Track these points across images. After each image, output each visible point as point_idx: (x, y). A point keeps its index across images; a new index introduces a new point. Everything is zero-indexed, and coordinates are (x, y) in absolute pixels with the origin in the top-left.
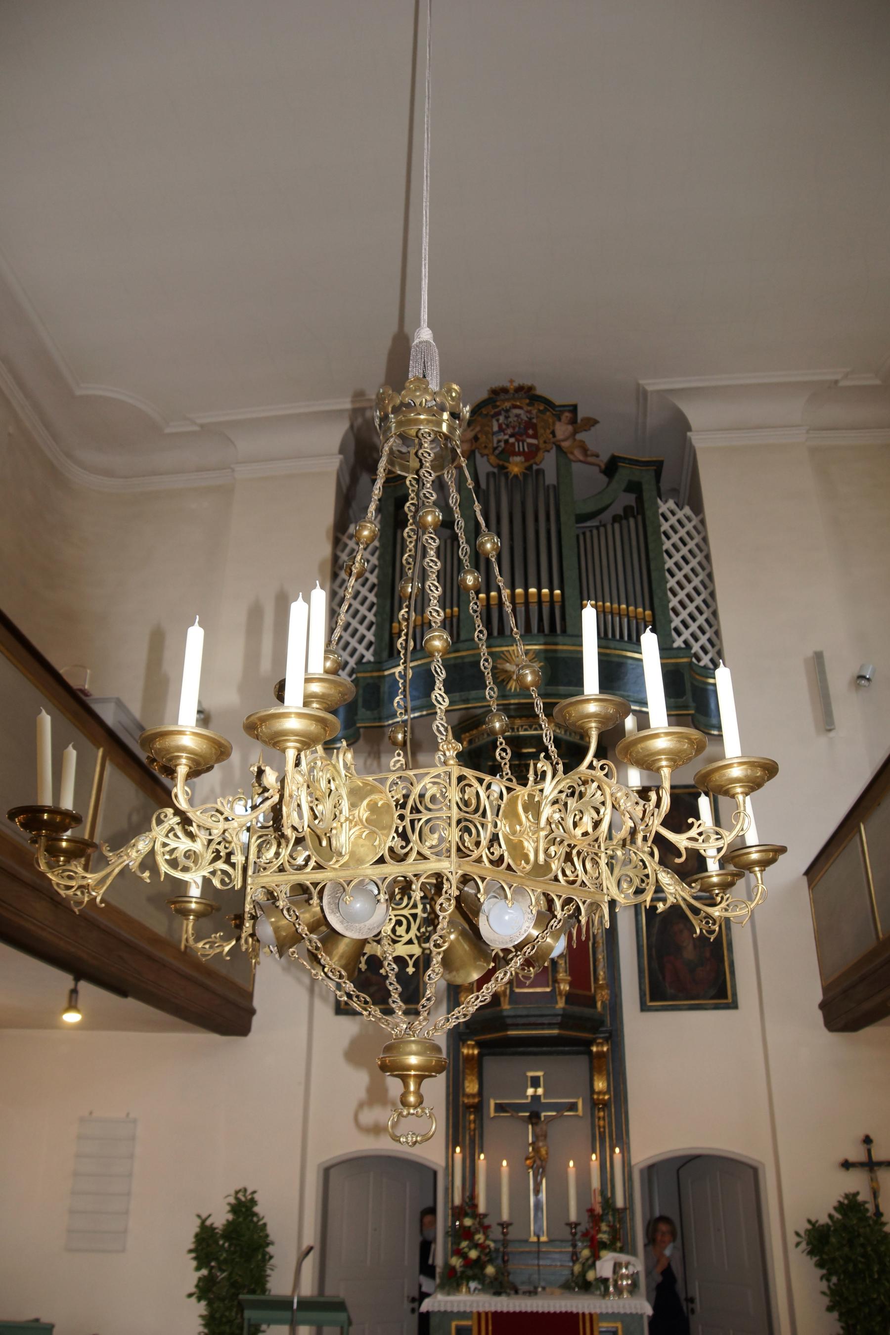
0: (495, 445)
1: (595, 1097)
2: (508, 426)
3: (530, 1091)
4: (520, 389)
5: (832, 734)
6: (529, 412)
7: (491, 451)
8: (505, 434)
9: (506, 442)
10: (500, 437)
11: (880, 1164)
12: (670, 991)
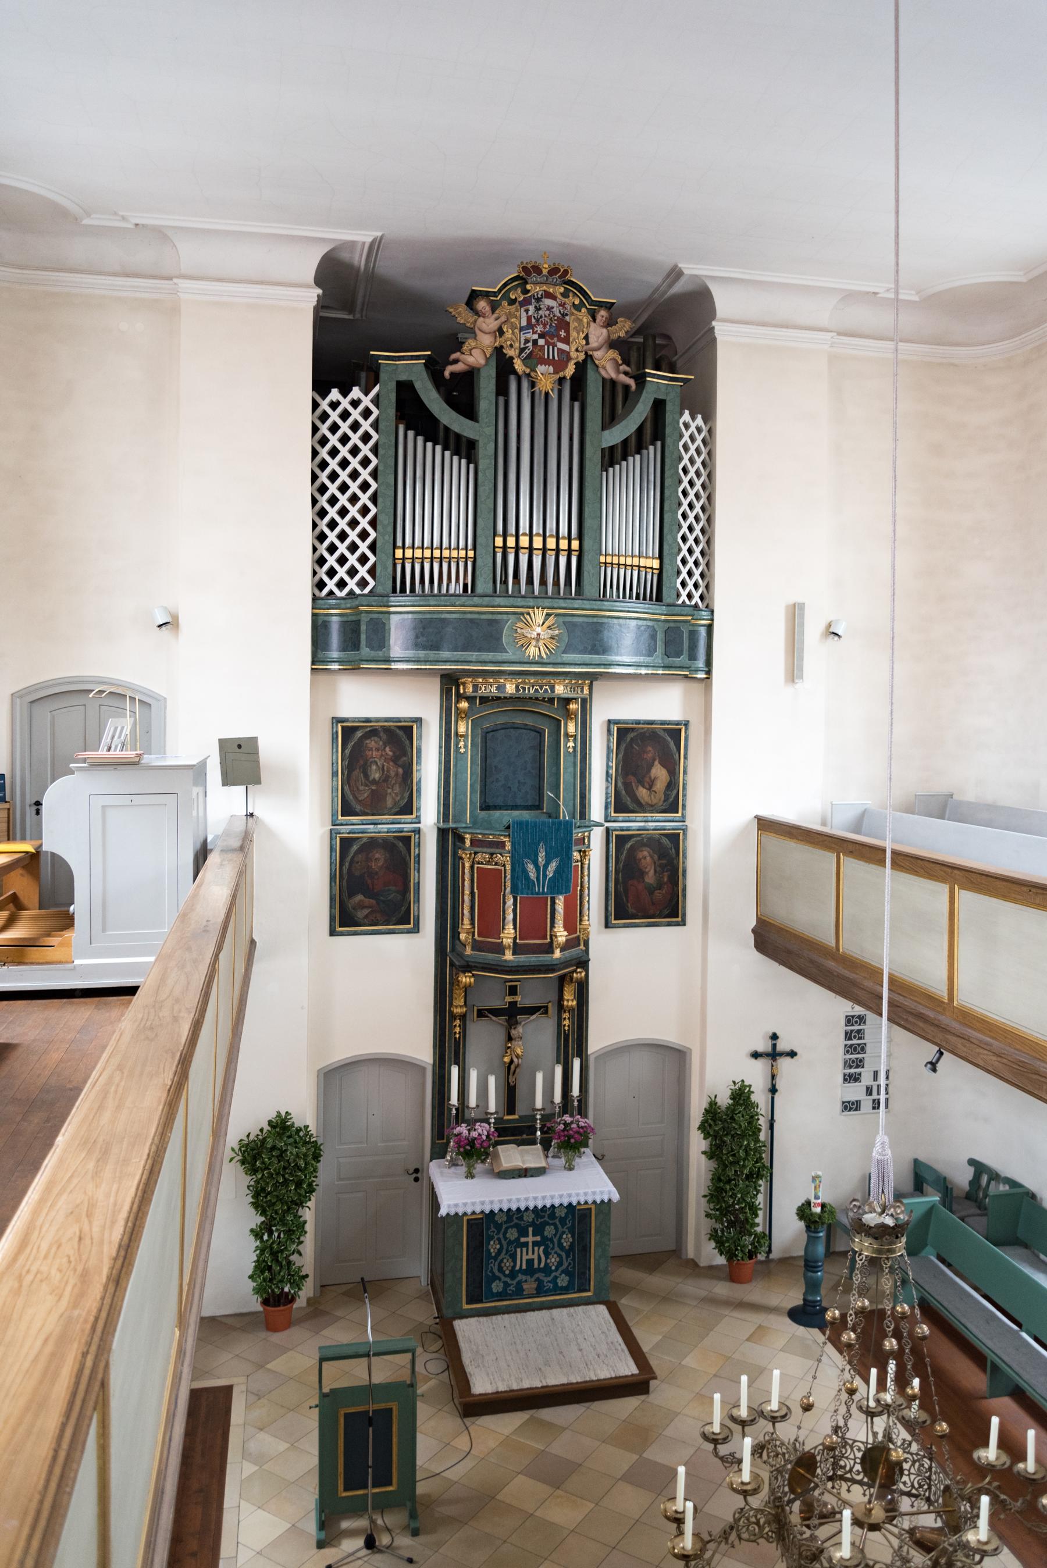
0: (522, 346)
1: (565, 1003)
2: (537, 320)
3: (508, 999)
4: (554, 271)
5: (799, 685)
6: (563, 305)
7: (517, 352)
8: (534, 333)
9: (535, 342)
10: (528, 336)
11: (782, 1054)
12: (631, 910)
